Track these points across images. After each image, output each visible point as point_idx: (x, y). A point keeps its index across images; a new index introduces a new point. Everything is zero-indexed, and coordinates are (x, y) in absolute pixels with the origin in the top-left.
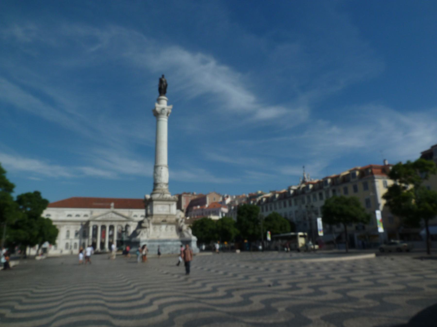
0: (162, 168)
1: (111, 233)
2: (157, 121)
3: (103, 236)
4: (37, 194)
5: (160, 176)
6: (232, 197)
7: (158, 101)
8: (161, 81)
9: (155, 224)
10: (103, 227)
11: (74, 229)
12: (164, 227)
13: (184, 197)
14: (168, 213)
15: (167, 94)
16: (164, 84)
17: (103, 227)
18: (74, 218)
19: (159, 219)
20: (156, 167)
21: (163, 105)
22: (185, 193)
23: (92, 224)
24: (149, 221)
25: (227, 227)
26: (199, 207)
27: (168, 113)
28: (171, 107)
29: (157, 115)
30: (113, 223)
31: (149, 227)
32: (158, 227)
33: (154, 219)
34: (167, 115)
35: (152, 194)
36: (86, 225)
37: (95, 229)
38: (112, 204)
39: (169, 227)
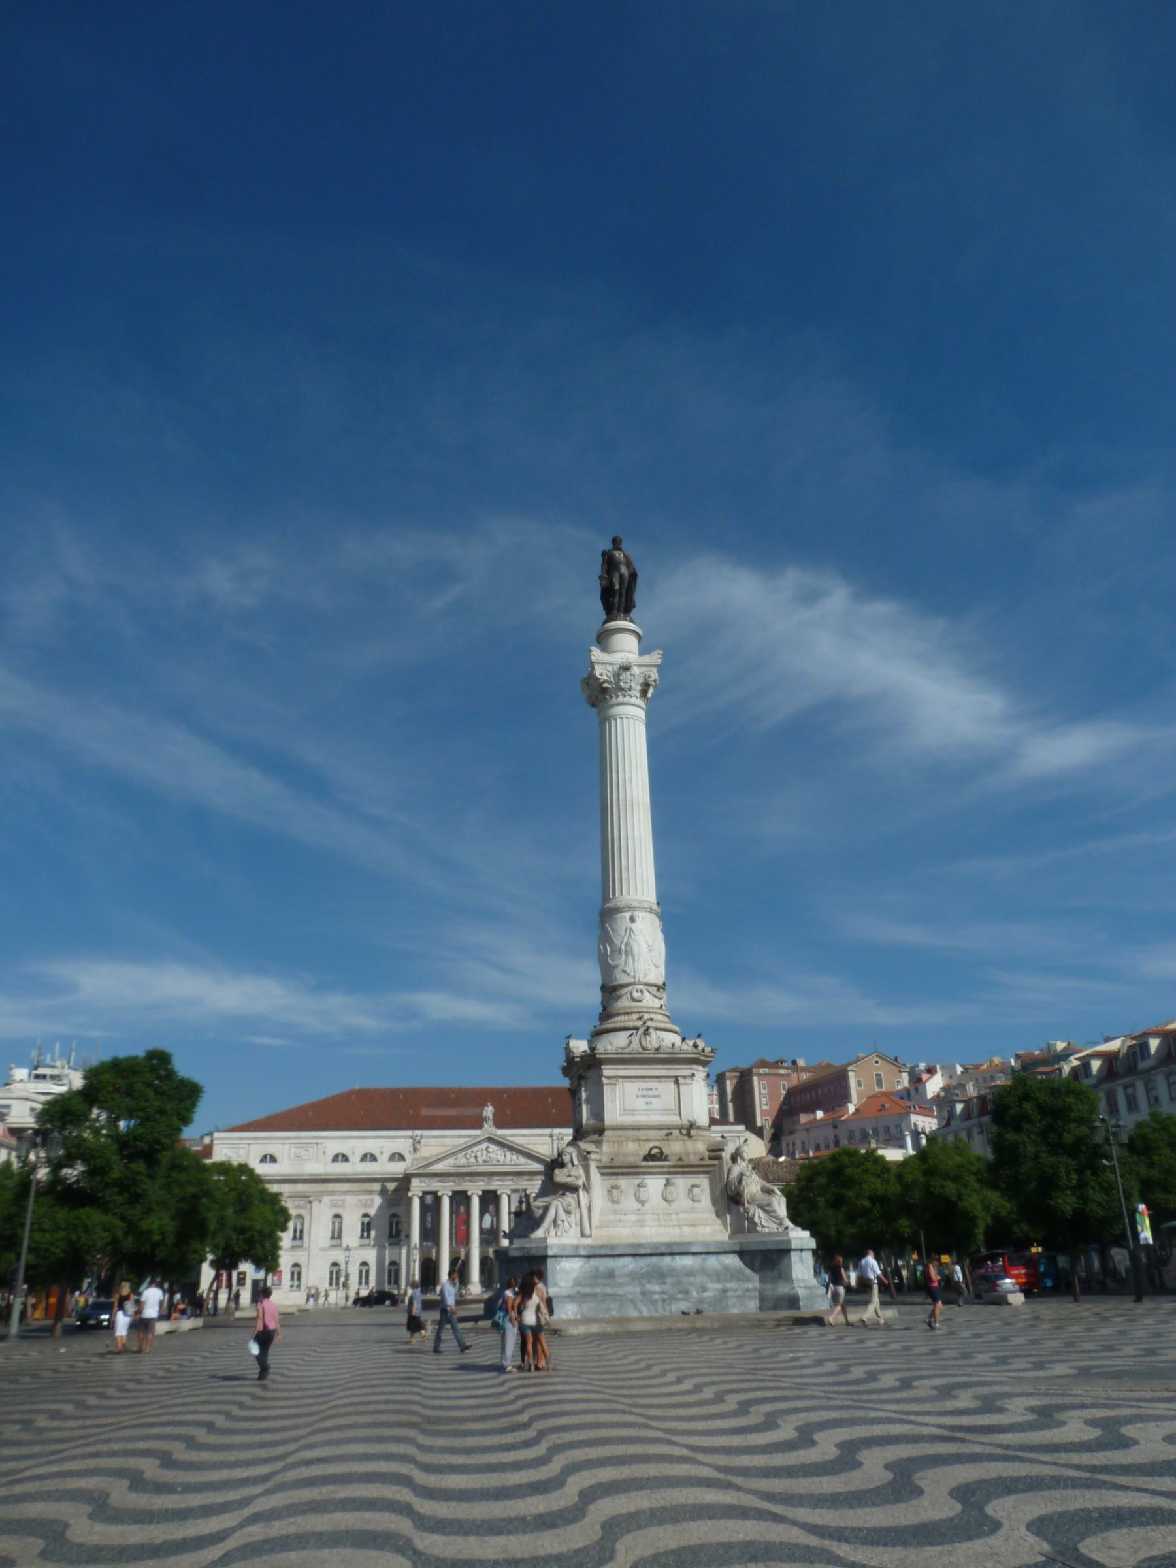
0: (632, 919)
1: (488, 1220)
2: (604, 720)
3: (461, 1236)
4: (159, 1060)
5: (629, 952)
6: (949, 1071)
7: (603, 639)
8: (610, 563)
9: (612, 1170)
10: (460, 1199)
11: (358, 1207)
12: (655, 1184)
13: (759, 1075)
14: (674, 1120)
15: (634, 613)
16: (624, 570)
17: (460, 1199)
19: (634, 1150)
20: (607, 914)
21: (625, 651)
22: (763, 1064)
23: (417, 1187)
24: (585, 1157)
25: (951, 1188)
26: (820, 1114)
27: (645, 687)
28: (655, 658)
29: (599, 696)
30: (495, 1184)
31: (587, 1188)
32: (623, 1182)
33: (607, 1149)
34: (644, 693)
35: (598, 1034)
36: (396, 1194)
37: (431, 1207)
38: (489, 1111)
39: (682, 1183)
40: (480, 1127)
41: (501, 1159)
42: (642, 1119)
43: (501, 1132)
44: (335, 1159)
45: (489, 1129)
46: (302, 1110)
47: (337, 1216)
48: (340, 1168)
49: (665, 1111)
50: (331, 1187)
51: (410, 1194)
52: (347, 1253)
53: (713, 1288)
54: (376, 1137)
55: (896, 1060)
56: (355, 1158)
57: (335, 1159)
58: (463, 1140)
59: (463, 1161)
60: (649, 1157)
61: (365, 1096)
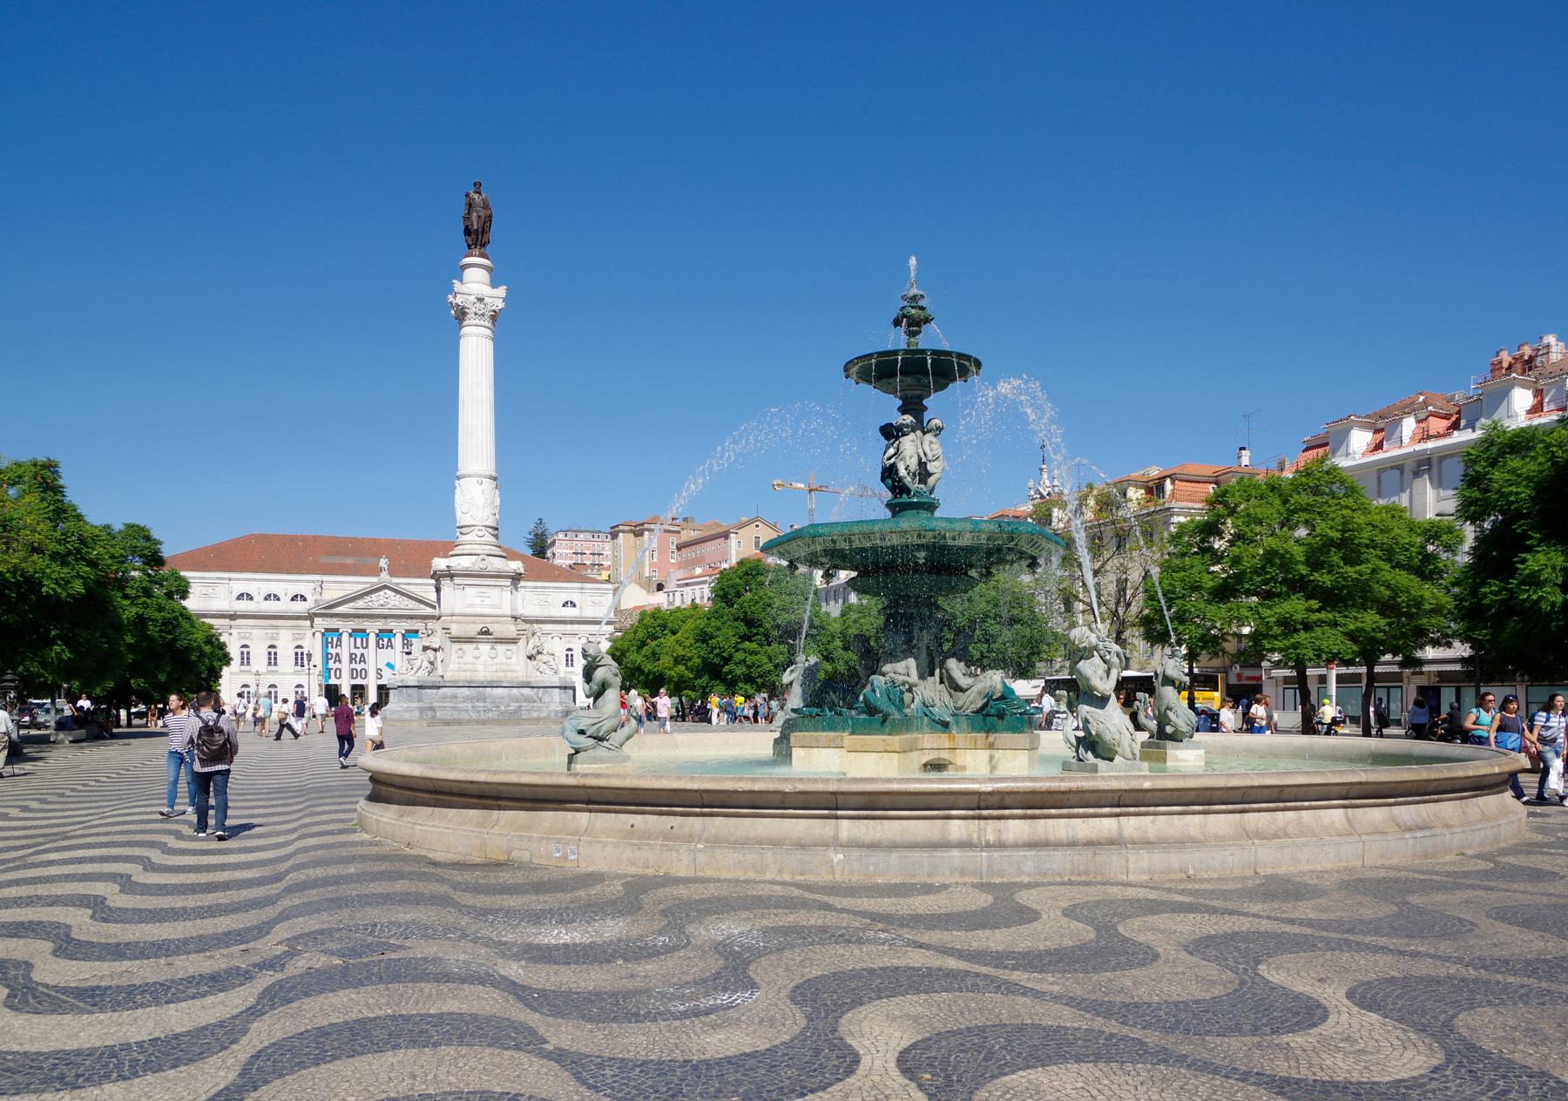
9: (457, 640)
12: (485, 648)
18: (259, 605)
19: (473, 629)
28: (502, 291)
32: (465, 646)
38: (383, 563)
40: (377, 571)
42: (478, 610)
43: (395, 580)
44: (240, 597)
45: (385, 576)
46: (204, 551)
47: (245, 646)
48: (244, 606)
49: (493, 606)
50: (239, 622)
53: (513, 706)
56: (258, 598)
57: (240, 597)
58: (360, 587)
60: (482, 633)
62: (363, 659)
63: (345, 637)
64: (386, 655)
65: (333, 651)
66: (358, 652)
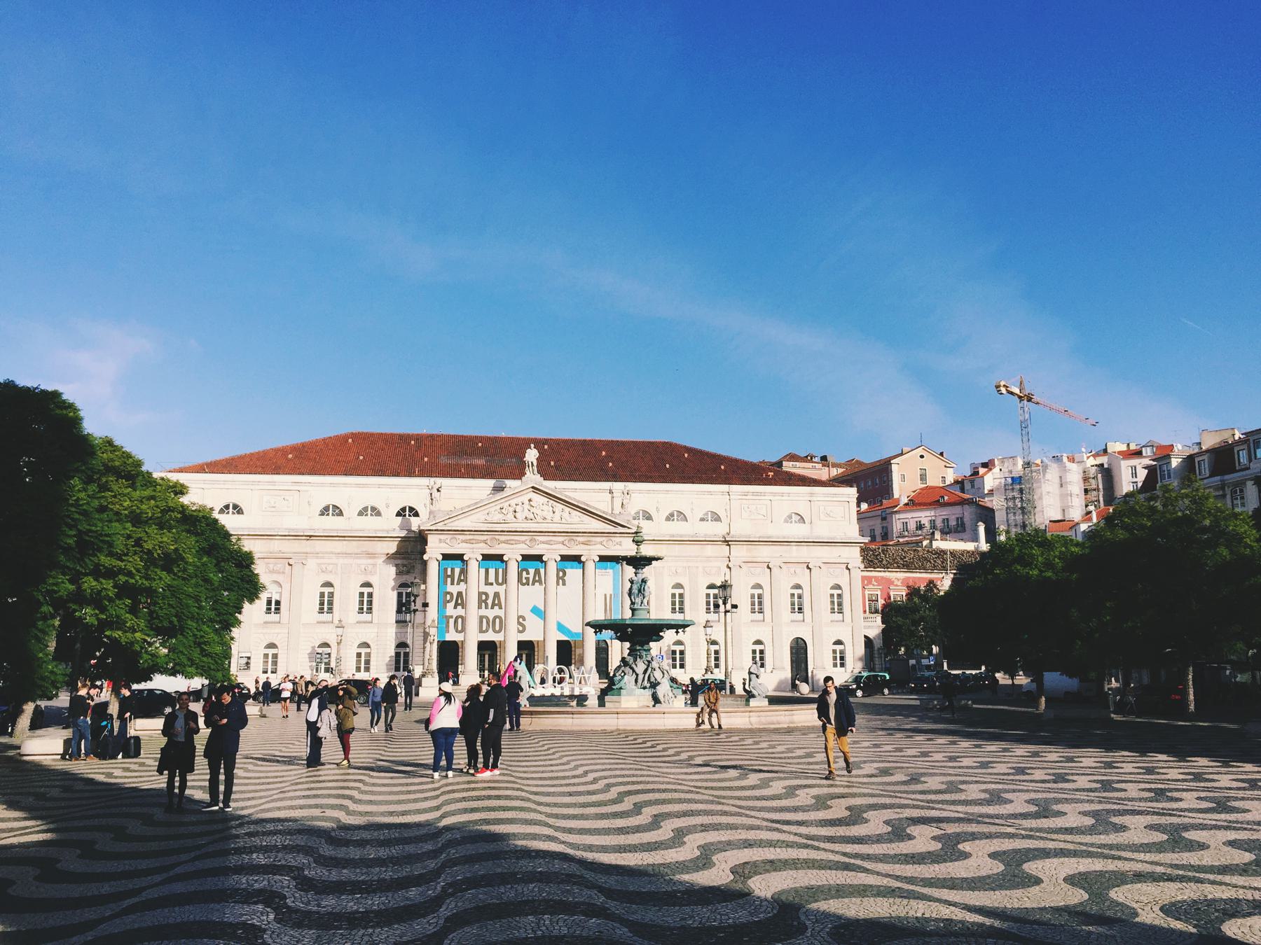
18: (351, 522)
38: (532, 455)
40: (518, 473)
41: (549, 515)
44: (325, 511)
51: (425, 557)
52: (340, 631)
54: (379, 486)
55: (942, 454)
56: (351, 511)
57: (325, 511)
59: (497, 517)
61: (363, 439)
62: (497, 603)
63: (473, 567)
64: (532, 595)
65: (454, 589)
66: (491, 590)
